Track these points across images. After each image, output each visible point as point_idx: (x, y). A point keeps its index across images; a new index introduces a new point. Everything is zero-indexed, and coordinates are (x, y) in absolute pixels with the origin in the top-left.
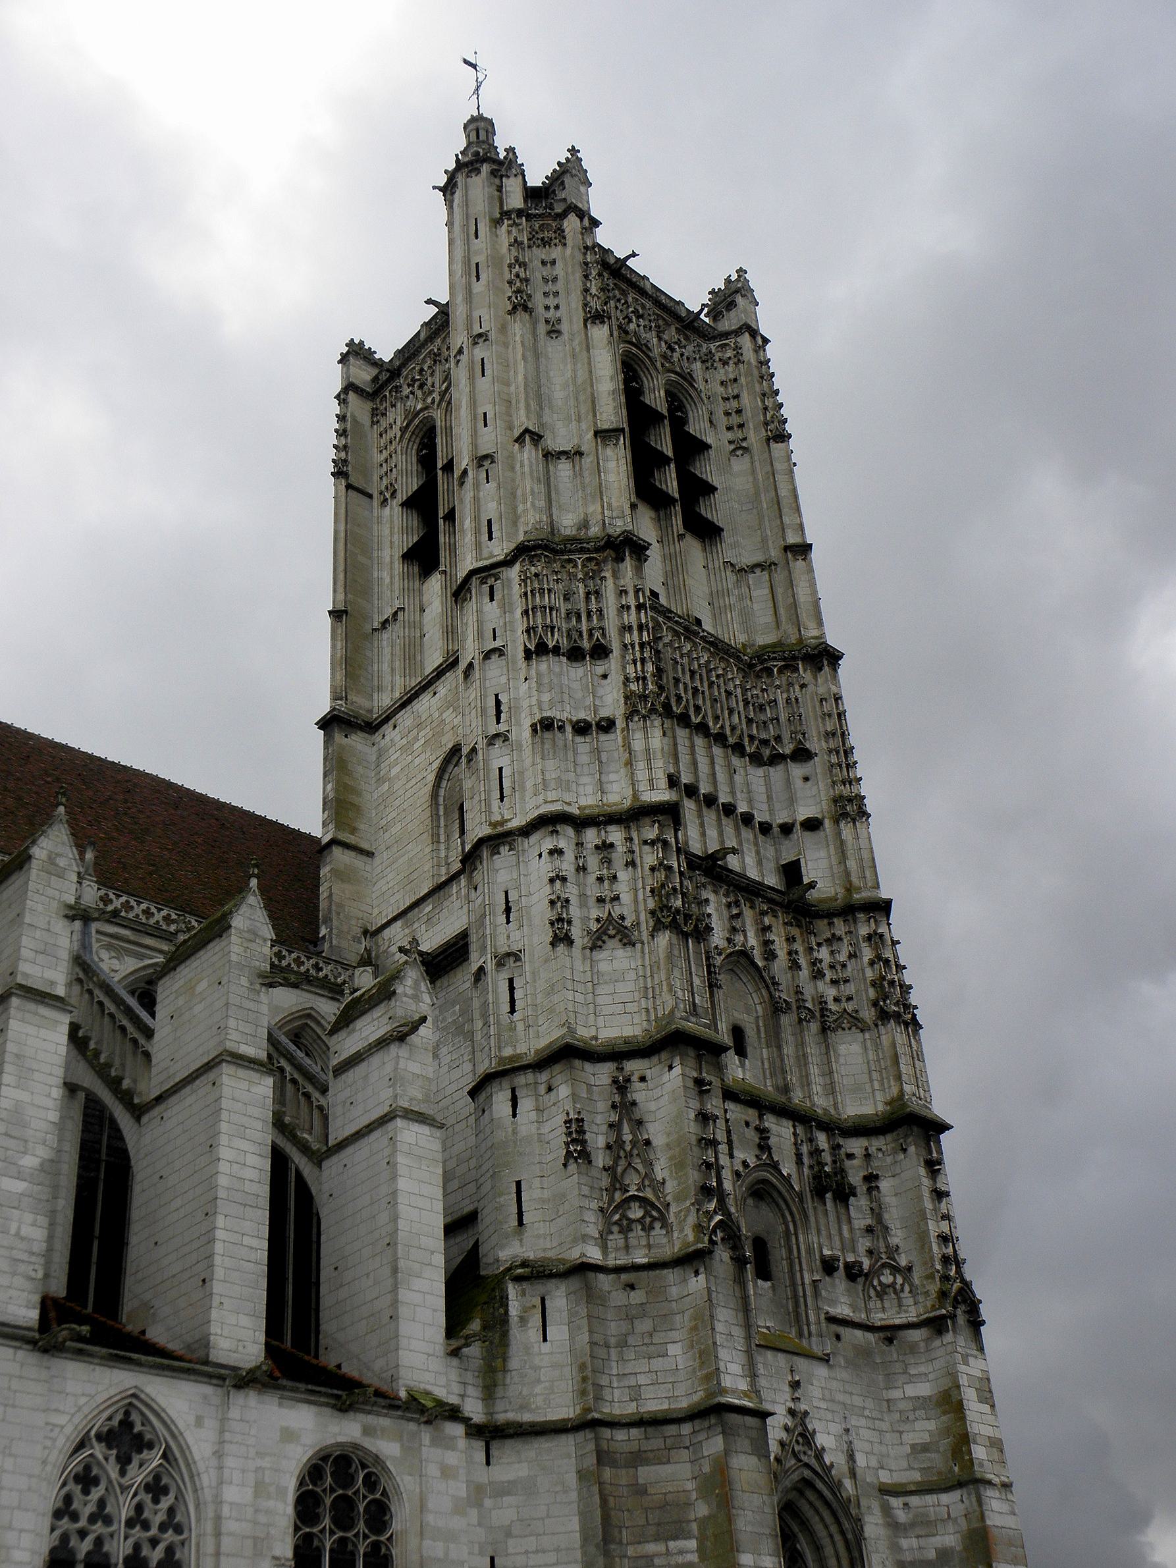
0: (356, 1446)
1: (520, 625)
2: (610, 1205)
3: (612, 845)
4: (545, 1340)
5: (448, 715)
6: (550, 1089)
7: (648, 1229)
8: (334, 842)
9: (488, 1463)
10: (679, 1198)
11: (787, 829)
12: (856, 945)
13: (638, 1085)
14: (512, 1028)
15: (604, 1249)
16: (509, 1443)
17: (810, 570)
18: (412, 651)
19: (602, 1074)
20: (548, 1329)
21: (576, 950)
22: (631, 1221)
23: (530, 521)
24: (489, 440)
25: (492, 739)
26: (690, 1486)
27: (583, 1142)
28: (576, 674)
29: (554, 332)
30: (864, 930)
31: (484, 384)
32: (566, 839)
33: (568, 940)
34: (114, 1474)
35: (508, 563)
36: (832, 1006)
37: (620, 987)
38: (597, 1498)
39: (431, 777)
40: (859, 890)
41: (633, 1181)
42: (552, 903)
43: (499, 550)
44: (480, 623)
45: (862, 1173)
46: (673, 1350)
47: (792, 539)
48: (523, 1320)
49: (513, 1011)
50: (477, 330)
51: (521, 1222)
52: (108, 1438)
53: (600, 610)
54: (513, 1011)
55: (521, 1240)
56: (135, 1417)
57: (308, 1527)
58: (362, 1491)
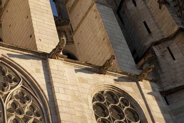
0: (113, 87)
2: (182, 15)
4: (174, 59)
9: (168, 104)
20: (174, 56)
48: (163, 56)
55: (152, 37)
57: (101, 104)
58: (122, 104)
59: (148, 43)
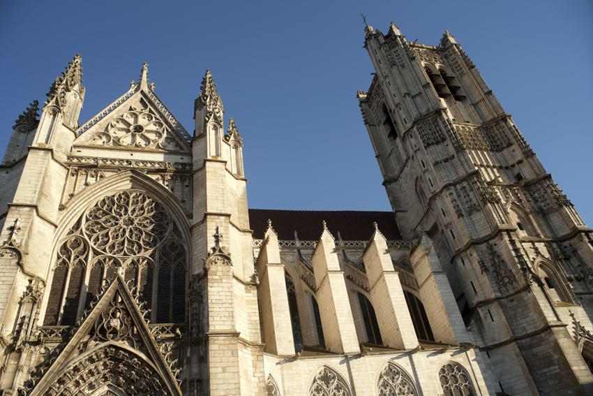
1: (421, 141)
3: (465, 187)
5: (413, 170)
6: (471, 255)
7: (511, 284)
8: (396, 212)
10: (517, 273)
11: (513, 166)
12: (545, 189)
13: (495, 247)
14: (456, 242)
15: (501, 292)
16: (493, 351)
17: (494, 96)
18: (399, 158)
19: (484, 246)
21: (465, 217)
22: (506, 283)
23: (415, 114)
24: (397, 100)
25: (424, 172)
26: (550, 350)
27: (485, 266)
28: (439, 147)
29: (403, 66)
30: (546, 185)
31: (391, 87)
32: (452, 189)
33: (462, 215)
34: (391, 383)
35: (412, 127)
36: (545, 208)
37: (481, 223)
38: (523, 360)
39: (414, 187)
40: (540, 175)
41: (502, 272)
42: (454, 207)
43: (409, 125)
44: (411, 144)
45: (571, 251)
46: (530, 314)
47: (486, 91)
48: (485, 317)
49: (454, 238)
50: (384, 75)
51: (476, 292)
52: (387, 374)
53: (440, 130)
54: (454, 238)
56: (391, 367)
59: (475, 300)
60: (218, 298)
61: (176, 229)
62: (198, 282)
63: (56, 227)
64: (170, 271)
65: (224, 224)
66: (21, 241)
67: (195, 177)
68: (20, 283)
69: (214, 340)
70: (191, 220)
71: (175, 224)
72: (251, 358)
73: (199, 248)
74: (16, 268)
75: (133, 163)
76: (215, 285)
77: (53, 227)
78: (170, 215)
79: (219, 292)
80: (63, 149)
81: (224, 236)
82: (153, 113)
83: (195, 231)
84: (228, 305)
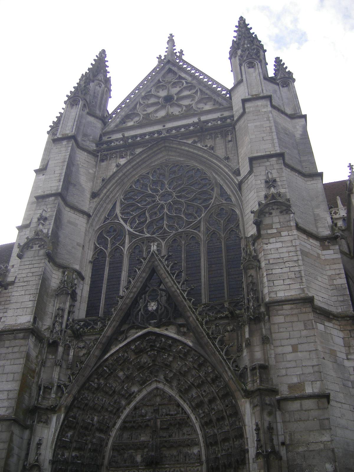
60: (277, 256)
61: (223, 193)
62: (253, 244)
63: (89, 216)
64: (221, 242)
65: (276, 167)
66: (48, 231)
67: (237, 127)
68: (54, 276)
69: (277, 311)
70: (238, 178)
71: (221, 188)
72: (341, 334)
73: (250, 205)
74: (43, 257)
75: (164, 132)
76: (272, 240)
77: (85, 217)
78: (215, 178)
79: (277, 249)
80: (91, 137)
81: (278, 179)
82: (184, 79)
83: (244, 187)
84: (291, 264)
